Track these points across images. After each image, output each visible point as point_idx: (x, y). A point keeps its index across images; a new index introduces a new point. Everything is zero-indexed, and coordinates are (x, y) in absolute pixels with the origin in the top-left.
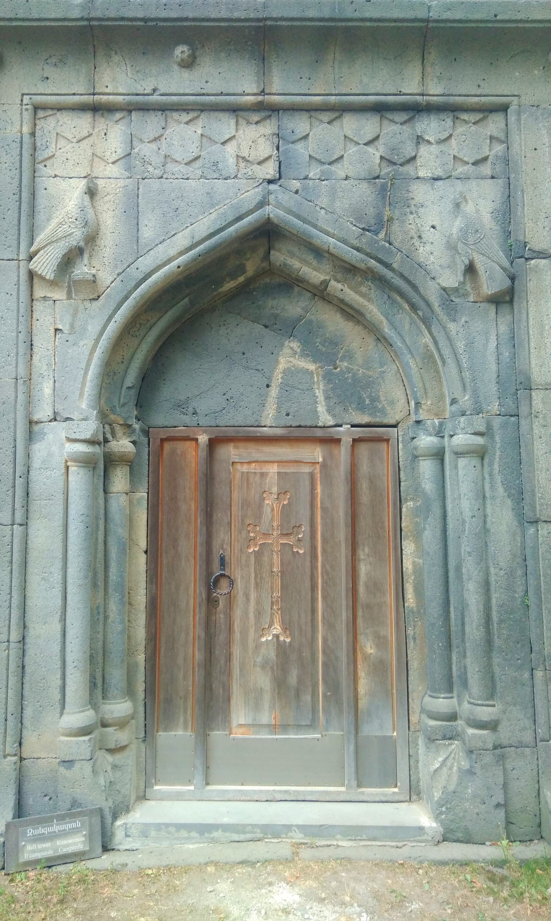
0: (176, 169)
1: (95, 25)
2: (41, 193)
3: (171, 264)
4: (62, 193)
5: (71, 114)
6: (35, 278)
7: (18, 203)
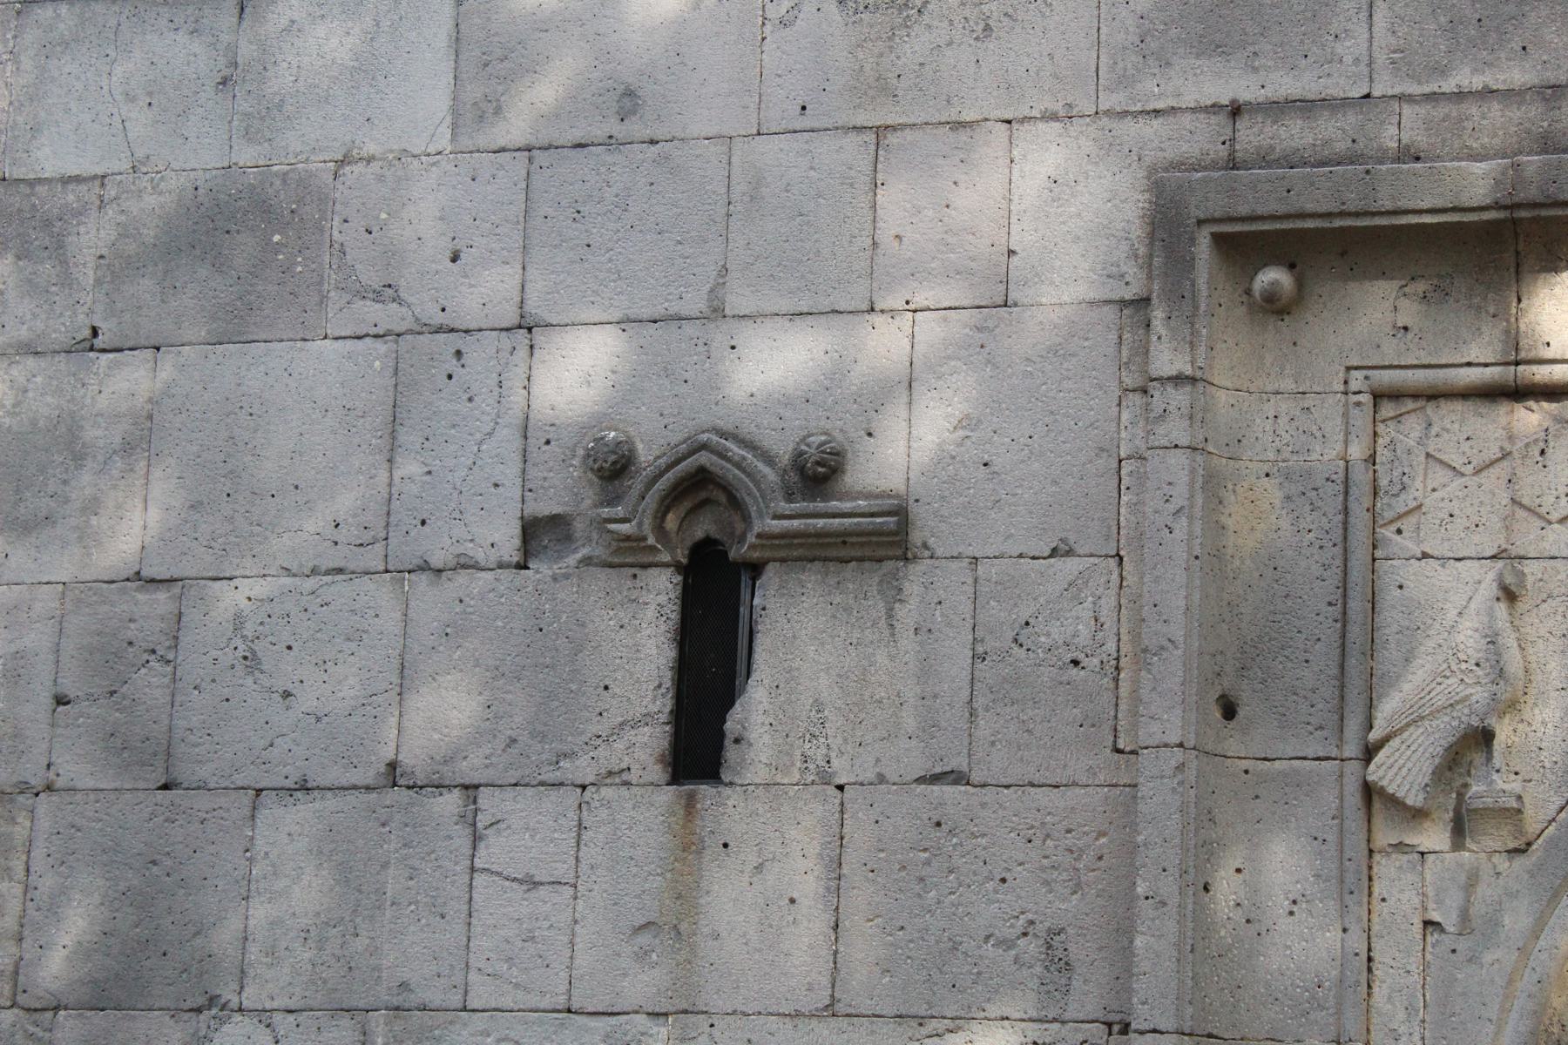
1: (1522, 219)
2: (1389, 596)
4: (1440, 596)
5: (1458, 406)
6: (1375, 798)
7: (1339, 625)
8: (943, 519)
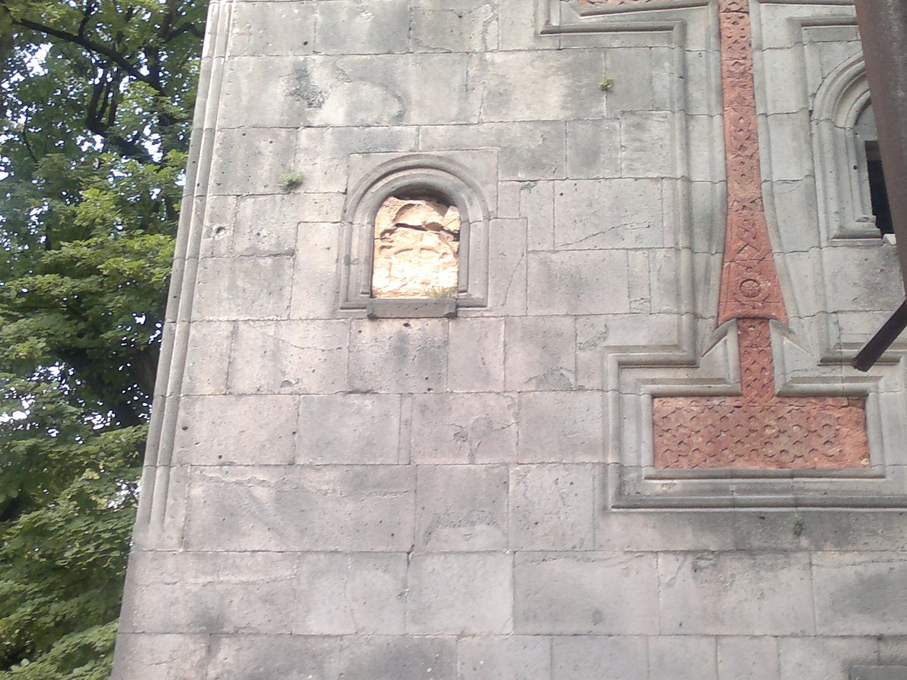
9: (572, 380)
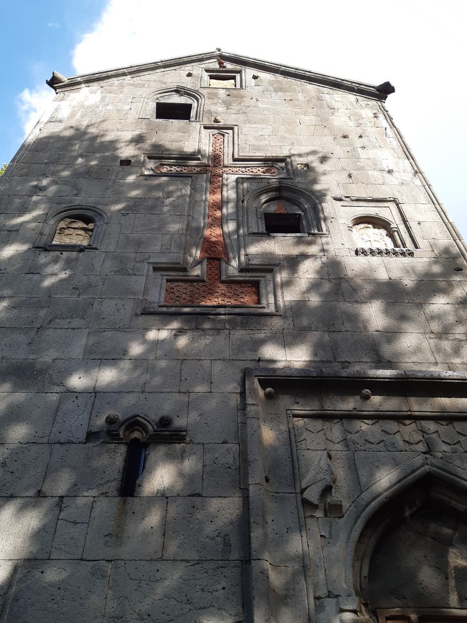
0: (372, 446)
3: (381, 496)
8: (196, 435)
9: (131, 272)
